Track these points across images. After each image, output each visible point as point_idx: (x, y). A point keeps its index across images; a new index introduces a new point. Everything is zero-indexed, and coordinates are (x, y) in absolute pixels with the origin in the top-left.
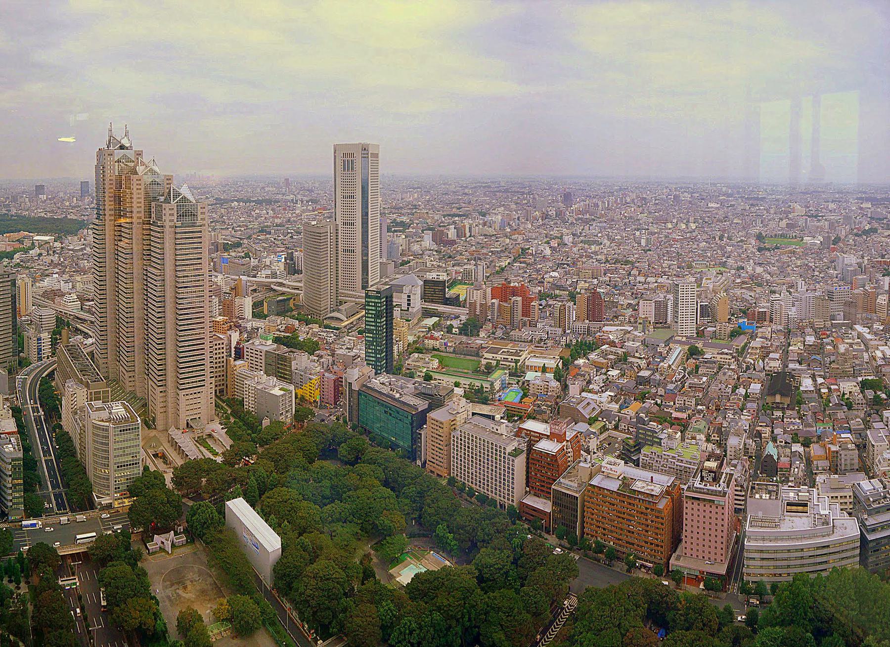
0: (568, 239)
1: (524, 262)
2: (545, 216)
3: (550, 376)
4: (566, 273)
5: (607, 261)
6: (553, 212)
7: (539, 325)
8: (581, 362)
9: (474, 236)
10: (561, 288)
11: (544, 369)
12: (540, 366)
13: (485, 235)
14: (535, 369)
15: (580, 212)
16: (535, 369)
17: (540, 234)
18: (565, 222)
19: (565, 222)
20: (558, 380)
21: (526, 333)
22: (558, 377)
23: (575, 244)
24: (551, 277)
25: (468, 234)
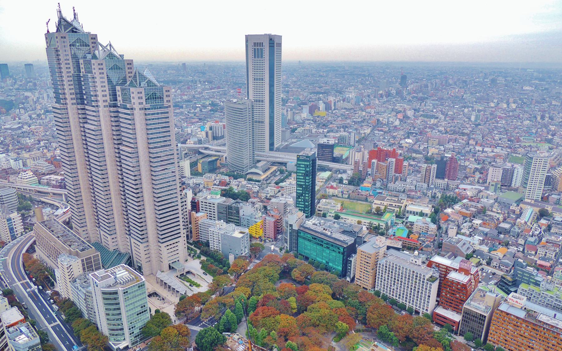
0: (410, 113)
1: (382, 131)
2: (388, 94)
3: (428, 220)
4: (418, 140)
5: (446, 132)
6: (394, 92)
7: (408, 180)
8: (449, 211)
9: (337, 109)
10: (417, 152)
11: (422, 214)
12: (419, 211)
13: (345, 109)
14: (415, 213)
15: (415, 92)
16: (415, 213)
17: (388, 108)
18: (403, 99)
19: (403, 99)
20: (434, 223)
21: (399, 185)
22: (434, 221)
23: (416, 117)
24: (407, 143)
25: (333, 108)
